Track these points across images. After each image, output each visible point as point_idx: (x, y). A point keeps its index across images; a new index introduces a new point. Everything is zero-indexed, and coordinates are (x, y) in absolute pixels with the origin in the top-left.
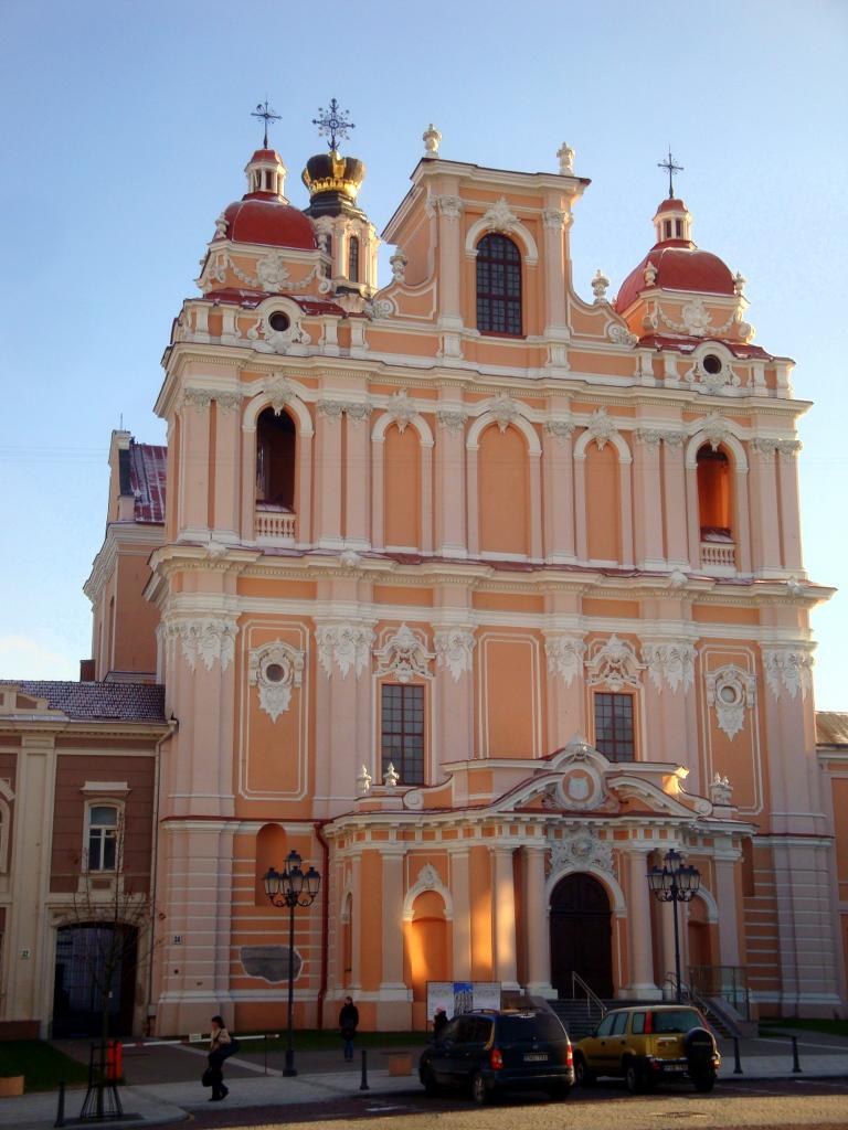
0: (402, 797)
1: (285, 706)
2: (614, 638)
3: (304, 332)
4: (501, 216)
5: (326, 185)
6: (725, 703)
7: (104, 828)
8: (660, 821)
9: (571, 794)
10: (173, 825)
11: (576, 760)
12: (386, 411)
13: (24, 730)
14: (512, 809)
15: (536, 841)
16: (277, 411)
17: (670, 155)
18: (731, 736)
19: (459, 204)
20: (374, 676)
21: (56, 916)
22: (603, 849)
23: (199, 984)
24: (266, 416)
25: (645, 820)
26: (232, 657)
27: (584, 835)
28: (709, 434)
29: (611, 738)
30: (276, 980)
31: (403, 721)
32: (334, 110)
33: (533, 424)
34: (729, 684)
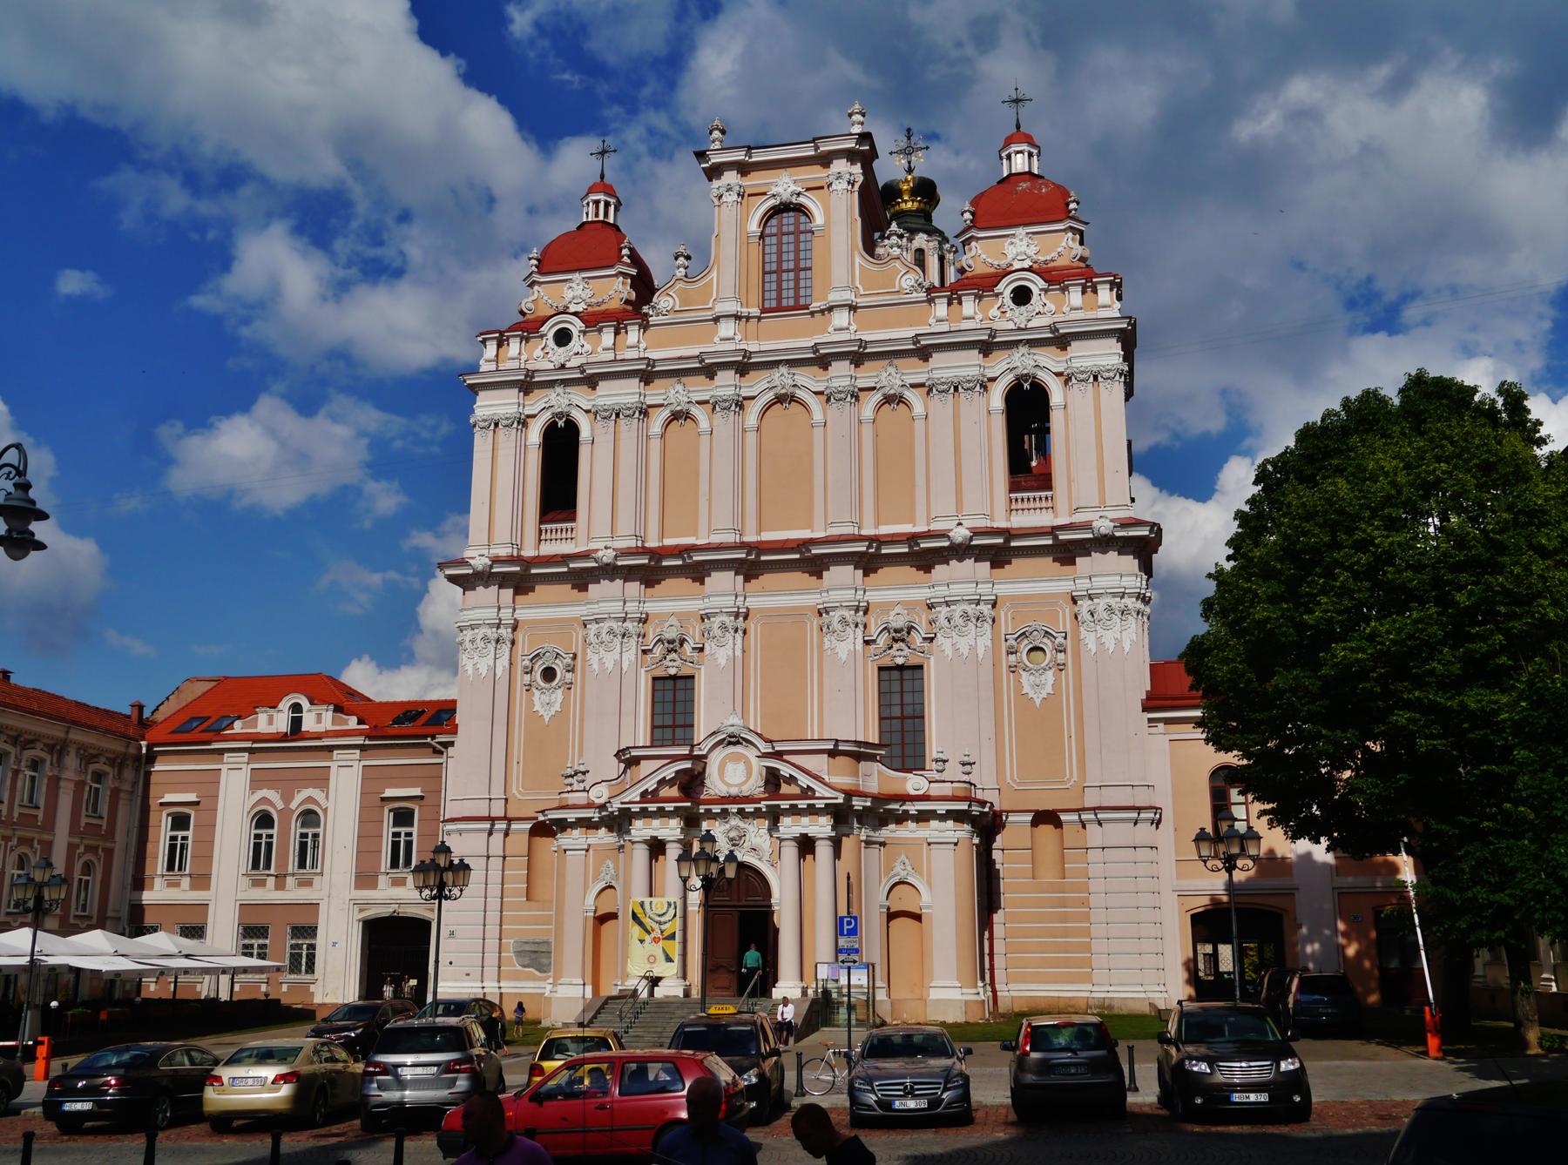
1: (557, 707)
2: (898, 609)
3: (585, 344)
4: (784, 185)
5: (897, 208)
6: (1031, 666)
7: (403, 830)
8: (802, 804)
10: (449, 827)
11: (730, 743)
12: (661, 405)
13: (333, 746)
14: (638, 799)
15: (670, 830)
16: (561, 423)
17: (1017, 89)
18: (1038, 702)
19: (737, 188)
21: (361, 911)
22: (761, 837)
23: (468, 975)
24: (551, 432)
25: (785, 804)
26: (507, 664)
27: (735, 822)
28: (1019, 372)
30: (545, 972)
32: (909, 138)
33: (816, 393)
34: (1037, 644)
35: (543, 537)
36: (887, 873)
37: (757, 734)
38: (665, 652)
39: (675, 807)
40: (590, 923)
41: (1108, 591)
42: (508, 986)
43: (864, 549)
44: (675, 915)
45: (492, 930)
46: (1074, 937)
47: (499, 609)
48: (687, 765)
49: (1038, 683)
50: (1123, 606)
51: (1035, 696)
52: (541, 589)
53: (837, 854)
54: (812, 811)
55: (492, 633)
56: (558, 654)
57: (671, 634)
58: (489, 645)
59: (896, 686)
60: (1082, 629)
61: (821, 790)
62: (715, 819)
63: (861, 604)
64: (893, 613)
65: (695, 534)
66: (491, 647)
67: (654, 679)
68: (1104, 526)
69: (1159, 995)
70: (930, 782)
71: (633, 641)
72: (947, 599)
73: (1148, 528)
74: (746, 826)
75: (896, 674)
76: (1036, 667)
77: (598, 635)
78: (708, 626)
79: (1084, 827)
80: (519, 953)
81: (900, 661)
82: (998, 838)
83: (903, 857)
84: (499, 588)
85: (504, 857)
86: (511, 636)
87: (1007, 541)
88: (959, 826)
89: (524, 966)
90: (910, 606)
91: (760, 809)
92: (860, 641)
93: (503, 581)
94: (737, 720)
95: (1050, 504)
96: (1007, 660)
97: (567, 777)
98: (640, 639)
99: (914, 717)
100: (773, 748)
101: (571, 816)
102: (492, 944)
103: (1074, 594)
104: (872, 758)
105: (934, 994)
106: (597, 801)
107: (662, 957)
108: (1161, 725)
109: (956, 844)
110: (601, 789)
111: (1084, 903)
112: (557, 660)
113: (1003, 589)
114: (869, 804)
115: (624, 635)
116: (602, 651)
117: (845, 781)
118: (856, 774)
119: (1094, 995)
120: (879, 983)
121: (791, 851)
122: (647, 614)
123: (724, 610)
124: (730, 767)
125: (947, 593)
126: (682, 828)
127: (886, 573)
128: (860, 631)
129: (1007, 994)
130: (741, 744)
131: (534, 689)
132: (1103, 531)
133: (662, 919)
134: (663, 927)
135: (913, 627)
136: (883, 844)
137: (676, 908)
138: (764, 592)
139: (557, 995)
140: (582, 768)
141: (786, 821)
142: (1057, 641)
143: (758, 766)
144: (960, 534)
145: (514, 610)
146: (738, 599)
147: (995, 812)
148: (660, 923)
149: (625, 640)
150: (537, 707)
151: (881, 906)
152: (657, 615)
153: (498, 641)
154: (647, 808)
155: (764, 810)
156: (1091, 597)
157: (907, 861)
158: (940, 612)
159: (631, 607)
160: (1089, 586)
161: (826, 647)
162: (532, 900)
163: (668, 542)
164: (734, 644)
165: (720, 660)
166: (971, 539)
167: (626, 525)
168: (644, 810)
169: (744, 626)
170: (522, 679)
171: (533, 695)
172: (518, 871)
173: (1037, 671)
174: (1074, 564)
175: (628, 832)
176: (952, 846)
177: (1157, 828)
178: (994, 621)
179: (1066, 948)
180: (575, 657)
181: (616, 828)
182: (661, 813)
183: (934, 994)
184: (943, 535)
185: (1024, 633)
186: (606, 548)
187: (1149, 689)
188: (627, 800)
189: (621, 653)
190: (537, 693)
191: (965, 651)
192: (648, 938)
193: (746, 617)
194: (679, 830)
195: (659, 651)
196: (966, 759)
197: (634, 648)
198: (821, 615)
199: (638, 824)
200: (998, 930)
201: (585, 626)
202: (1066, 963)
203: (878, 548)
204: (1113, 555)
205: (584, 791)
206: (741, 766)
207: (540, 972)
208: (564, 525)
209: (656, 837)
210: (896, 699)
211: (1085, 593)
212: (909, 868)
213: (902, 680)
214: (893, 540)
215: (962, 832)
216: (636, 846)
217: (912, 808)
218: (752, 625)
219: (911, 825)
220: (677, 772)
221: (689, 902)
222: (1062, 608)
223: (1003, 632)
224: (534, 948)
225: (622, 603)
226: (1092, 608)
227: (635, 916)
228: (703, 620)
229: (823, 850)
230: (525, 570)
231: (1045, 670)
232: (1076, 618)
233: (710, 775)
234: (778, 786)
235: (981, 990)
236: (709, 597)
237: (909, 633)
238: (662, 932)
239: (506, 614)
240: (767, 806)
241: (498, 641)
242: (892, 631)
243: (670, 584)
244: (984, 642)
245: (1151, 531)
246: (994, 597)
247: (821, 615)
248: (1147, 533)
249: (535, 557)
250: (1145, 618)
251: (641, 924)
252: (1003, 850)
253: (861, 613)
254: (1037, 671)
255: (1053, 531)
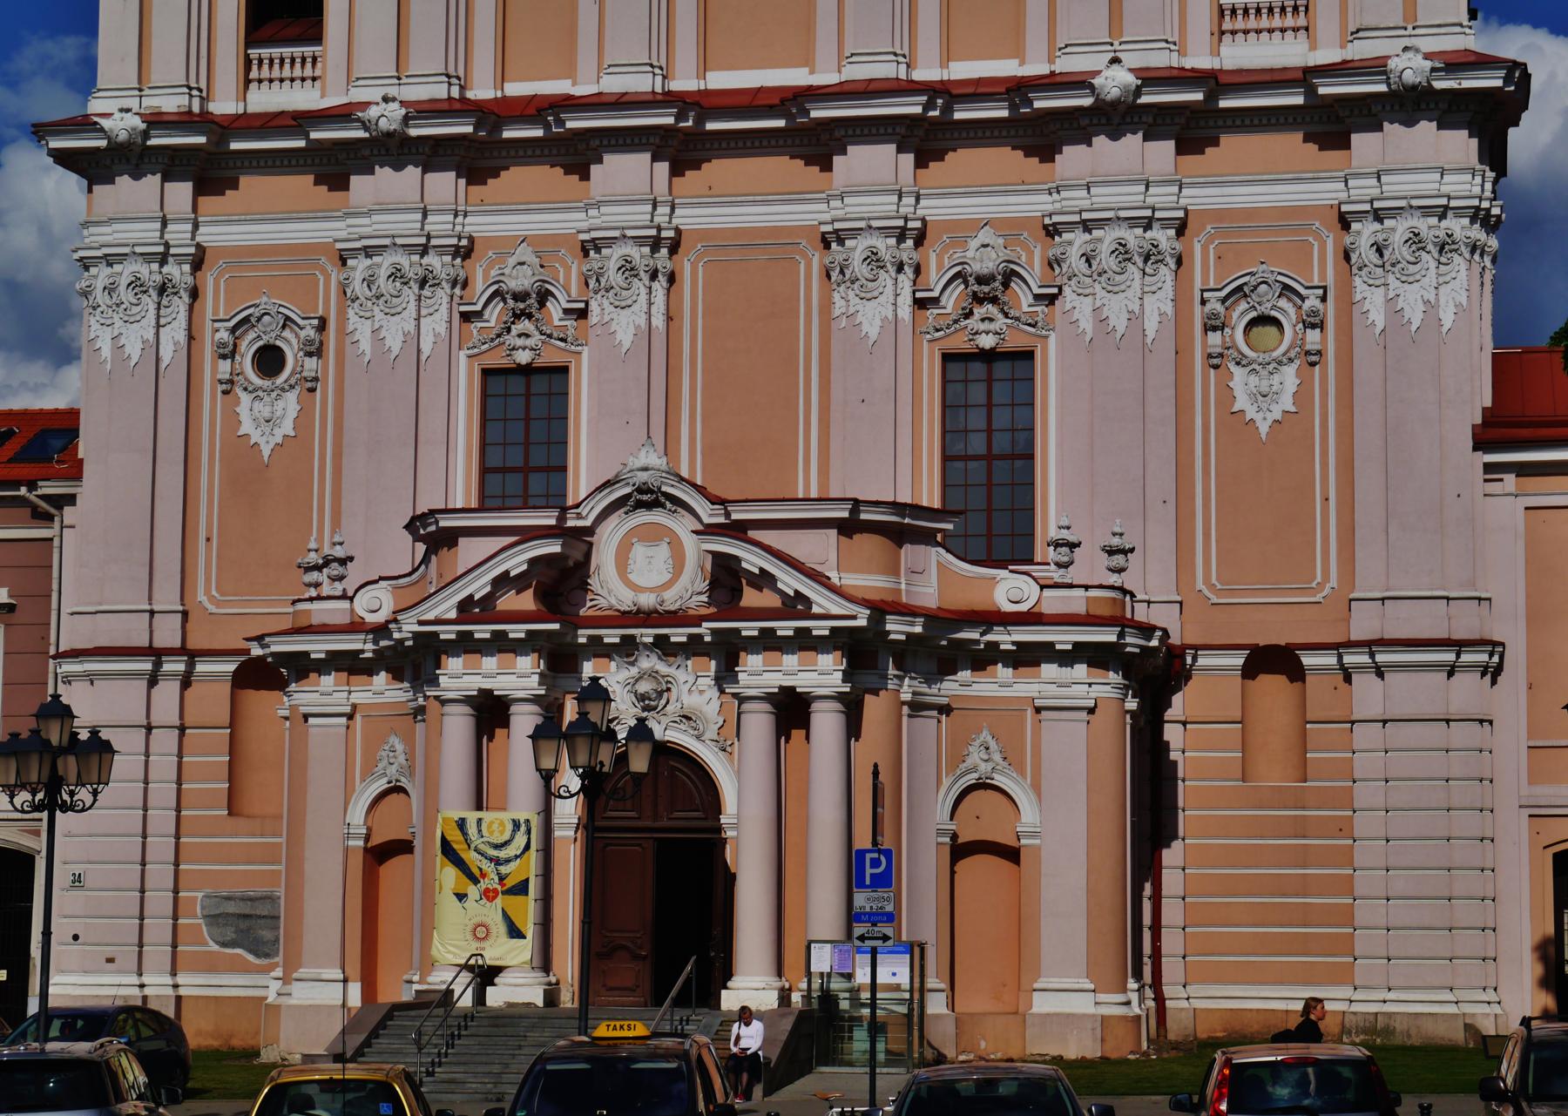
0: (351, 599)
1: (287, 428)
2: (985, 236)
8: (785, 628)
9: (629, 576)
10: (69, 667)
11: (640, 505)
14: (453, 615)
18: (1264, 428)
20: (463, 355)
22: (701, 692)
23: (110, 960)
25: (750, 629)
26: (182, 337)
27: (648, 662)
29: (982, 450)
30: (267, 956)
31: (527, 444)
34: (1265, 309)
35: (254, 74)
36: (952, 767)
37: (694, 486)
38: (507, 317)
39: (529, 632)
40: (357, 862)
41: (1415, 203)
42: (192, 984)
43: (918, 110)
44: (527, 847)
45: (160, 874)
46: (1320, 895)
47: (164, 223)
48: (554, 547)
49: (1265, 389)
50: (1442, 234)
51: (1258, 417)
52: (252, 185)
53: (853, 728)
54: (804, 642)
55: (149, 273)
56: (288, 318)
57: (521, 280)
58: (144, 298)
59: (978, 393)
60: (1358, 281)
61: (822, 601)
62: (609, 656)
63: (911, 225)
64: (974, 244)
65: (570, 73)
66: (149, 302)
67: (487, 373)
68: (1411, 68)
69: (1486, 1009)
70: (1042, 587)
71: (443, 294)
72: (1086, 216)
73: (1502, 73)
74: (671, 671)
75: (978, 369)
76: (1262, 357)
77: (369, 281)
78: (596, 266)
79: (1348, 679)
80: (213, 919)
81: (987, 342)
82: (1177, 699)
83: (985, 736)
84: (165, 179)
85: (182, 729)
86: (190, 280)
87: (1212, 97)
88: (1099, 675)
89: (224, 945)
90: (1009, 228)
91: (700, 636)
92: (906, 300)
93: (172, 165)
94: (654, 459)
95: (1302, 21)
96: (1204, 344)
97: (310, 569)
98: (457, 291)
99: (1013, 457)
100: (727, 515)
101: (318, 647)
102: (159, 901)
103: (1344, 208)
104: (927, 538)
105: (1042, 1004)
106: (371, 618)
107: (500, 928)
108: (1510, 479)
109: (1091, 711)
110: (374, 593)
111: (1344, 828)
112: (287, 333)
113: (1198, 198)
114: (918, 629)
115: (423, 283)
116: (379, 315)
117: (870, 582)
118: (895, 572)
119: (1356, 1008)
120: (932, 982)
121: (759, 723)
122: (471, 239)
123: (630, 233)
124: (639, 551)
125: (1086, 204)
126: (541, 675)
127: (963, 161)
128: (906, 281)
129: (1184, 1004)
130: (663, 506)
131: (238, 391)
132: (1409, 77)
133: (502, 854)
134: (504, 869)
135: (1015, 273)
136: (945, 710)
137: (529, 832)
138: (712, 196)
139: (293, 1001)
140: (339, 552)
141: (752, 662)
142: (1307, 305)
143: (695, 549)
144: (1115, 81)
145: (196, 226)
146: (660, 210)
147: (1170, 648)
148: (497, 862)
149: (426, 292)
150: (247, 427)
151: (940, 832)
152: (490, 241)
153: (162, 290)
154: (471, 633)
155: (708, 639)
156: (1378, 215)
157: (992, 744)
158: (1070, 243)
159: (439, 224)
160: (1376, 192)
161: (837, 312)
162: (237, 815)
163: (515, 89)
164: (650, 304)
165: (619, 336)
166: (1138, 92)
167: (427, 54)
168: (465, 637)
169: (669, 265)
170: (214, 370)
171: (238, 402)
172: (210, 757)
173: (1264, 365)
174: (1348, 147)
175: (434, 681)
176: (1084, 715)
177: (1494, 682)
178: (1179, 262)
179: (1305, 916)
180: (322, 325)
181: (408, 673)
182: (500, 645)
183: (1042, 1004)
184: (1080, 83)
185: (1239, 289)
186: (386, 99)
187: (1488, 403)
188: (430, 616)
189: (418, 319)
190: (245, 398)
191: (1119, 322)
192: (473, 891)
193: (674, 248)
194: (536, 678)
195: (495, 315)
196: (1116, 541)
197: (444, 309)
198: (827, 246)
199: (453, 664)
200: (1172, 881)
201: (344, 262)
202: (1303, 945)
203: (947, 110)
204: (1426, 128)
205: (344, 597)
206: (663, 551)
207: (257, 955)
208: (297, 51)
209: (490, 692)
210: (977, 419)
211: (1367, 207)
212: (997, 757)
213: (990, 381)
214: (979, 91)
215: (1105, 686)
216: (449, 709)
217: (1006, 638)
218: (685, 266)
219: (1003, 672)
220: (532, 562)
221: (555, 820)
222: (1318, 236)
223: (1198, 285)
224: (245, 909)
225: (419, 216)
226: (1380, 237)
227: (447, 849)
228: (586, 254)
229: (826, 723)
230: (218, 144)
231: (1280, 363)
232: (1347, 258)
233: (598, 567)
234: (737, 593)
235: (1134, 997)
236: (598, 204)
237: (1006, 285)
238: (502, 879)
239: (179, 234)
240: (714, 632)
241: (162, 290)
242: (971, 280)
243: (516, 178)
244: (1159, 305)
245: (1507, 80)
246: (1181, 214)
247: (827, 246)
248: (1499, 83)
249: (237, 117)
250: (1487, 261)
251: (459, 863)
252: (1184, 723)
253: (910, 243)
254: (1264, 365)
255: (1306, 77)
